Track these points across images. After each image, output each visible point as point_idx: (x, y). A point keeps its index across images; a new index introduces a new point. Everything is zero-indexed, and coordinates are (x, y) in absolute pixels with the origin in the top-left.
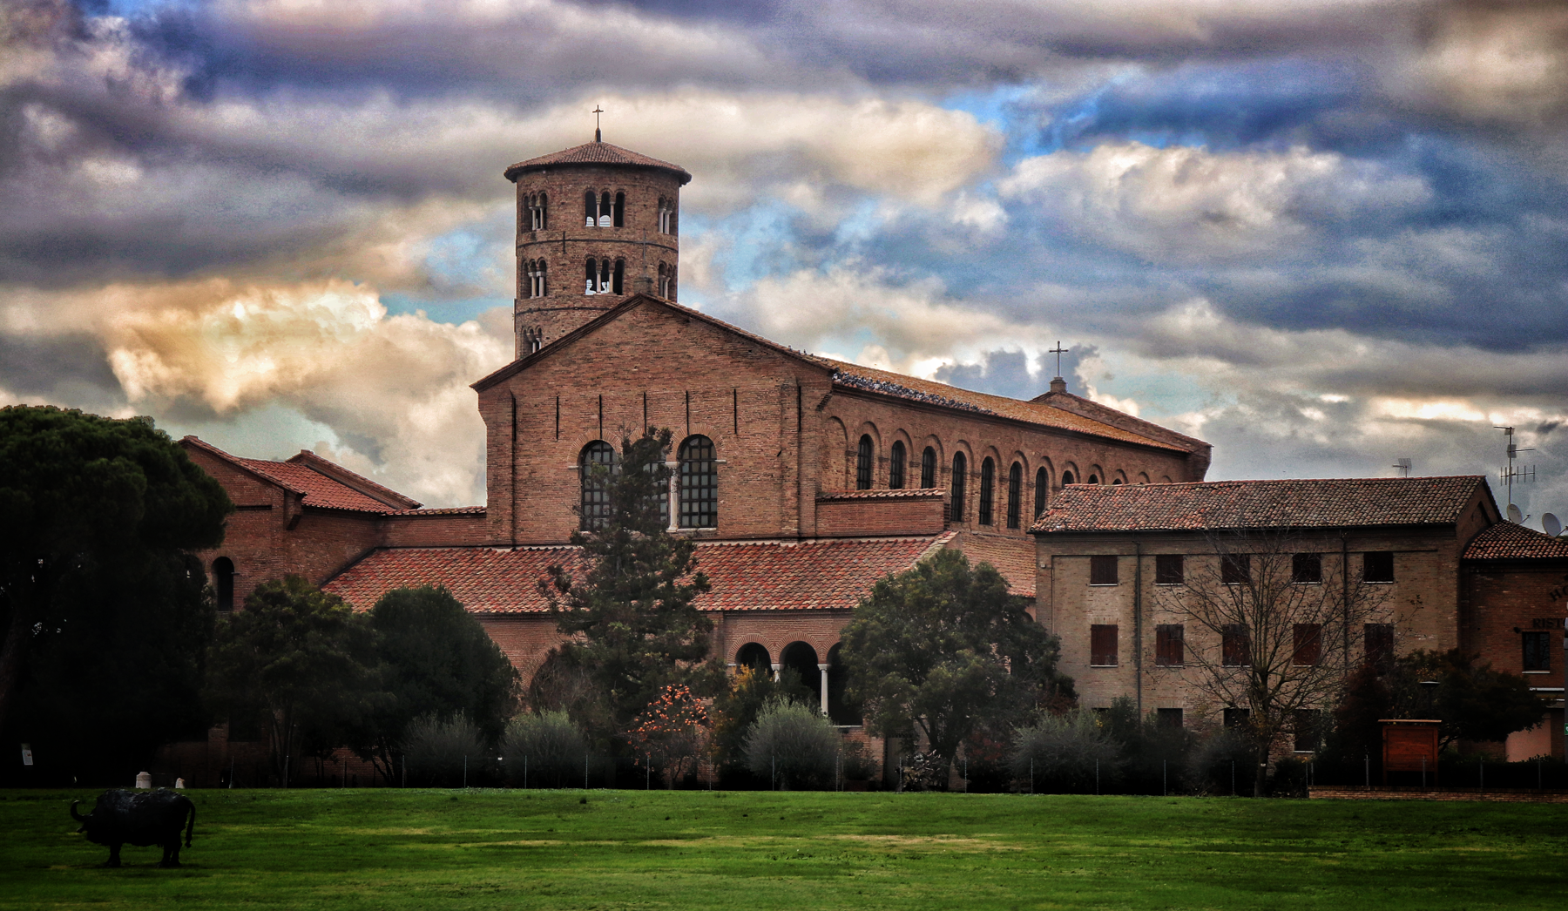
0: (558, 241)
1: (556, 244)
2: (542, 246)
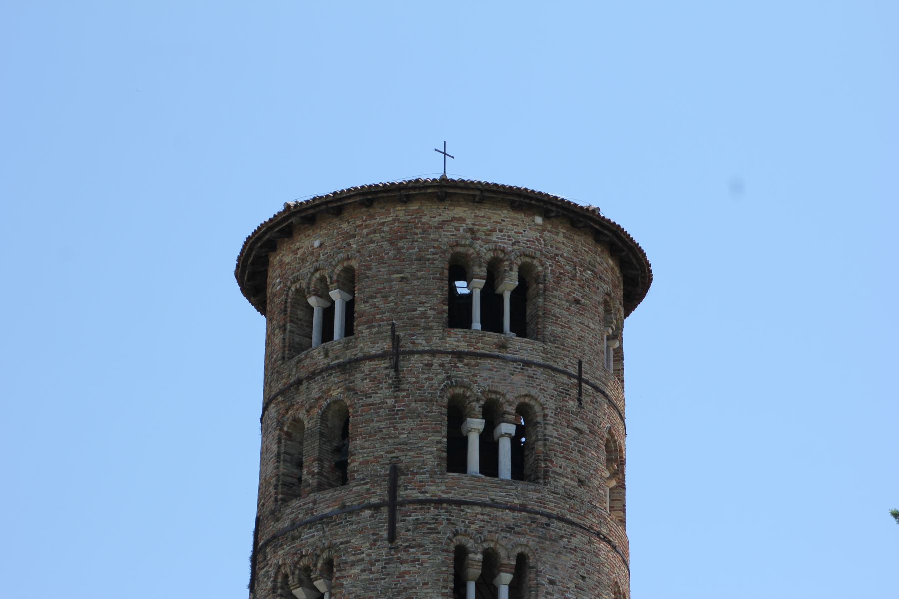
0: (570, 376)
1: (565, 379)
2: (530, 371)
